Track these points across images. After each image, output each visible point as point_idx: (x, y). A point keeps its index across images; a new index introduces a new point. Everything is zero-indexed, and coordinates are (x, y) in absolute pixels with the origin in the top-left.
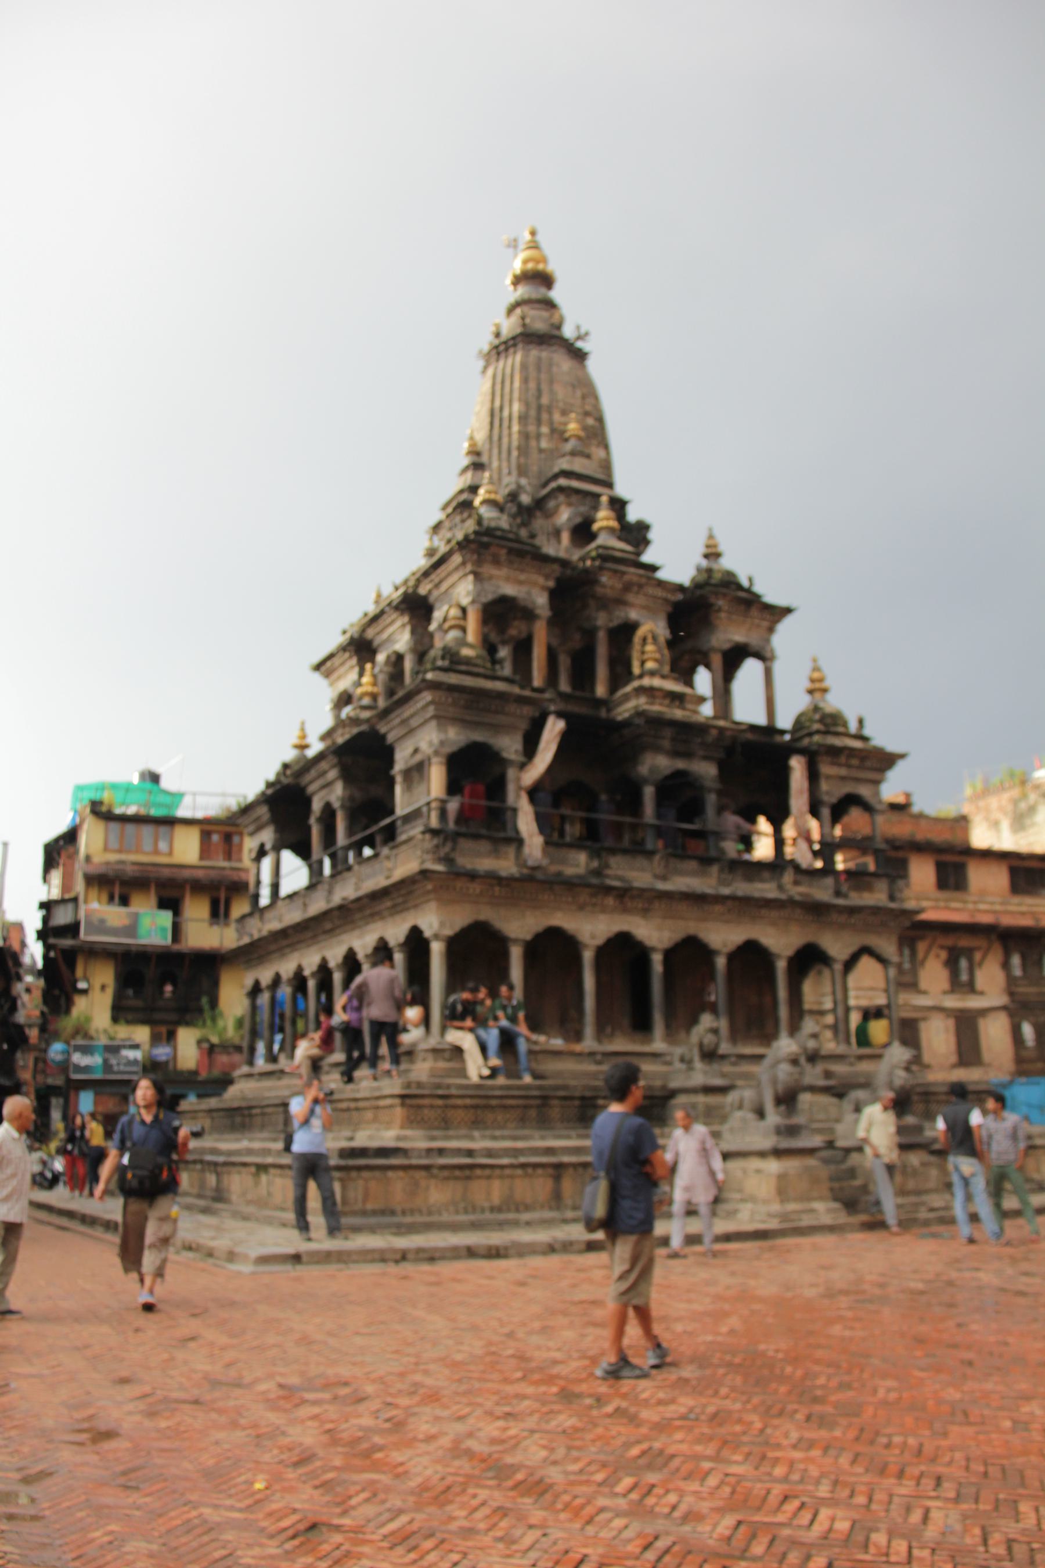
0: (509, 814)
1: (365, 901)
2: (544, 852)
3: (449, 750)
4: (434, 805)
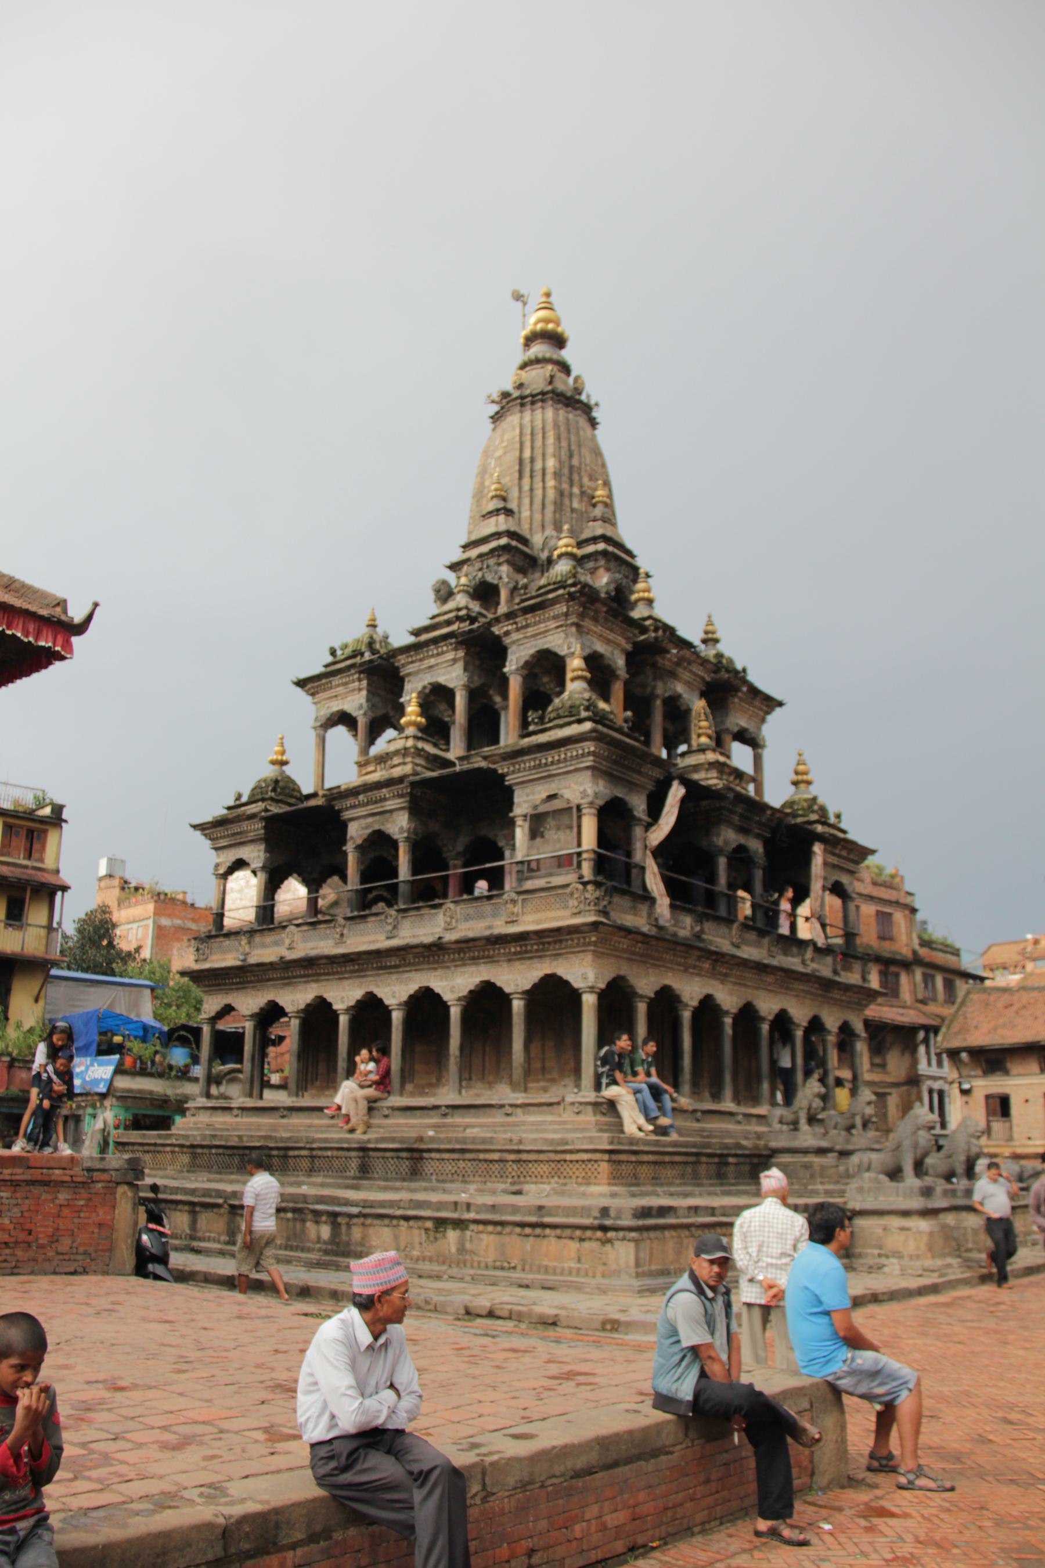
0: (634, 871)
1: (484, 942)
2: (671, 912)
3: (600, 802)
4: (585, 856)
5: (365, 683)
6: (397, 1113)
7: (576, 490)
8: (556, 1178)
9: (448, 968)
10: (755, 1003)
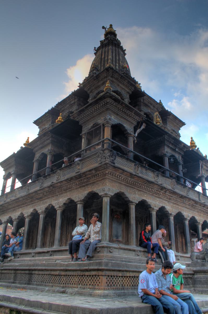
4: (105, 142)
5: (51, 119)
6: (37, 255)
7: (117, 64)
8: (81, 285)
9: (57, 195)
10: (182, 212)
